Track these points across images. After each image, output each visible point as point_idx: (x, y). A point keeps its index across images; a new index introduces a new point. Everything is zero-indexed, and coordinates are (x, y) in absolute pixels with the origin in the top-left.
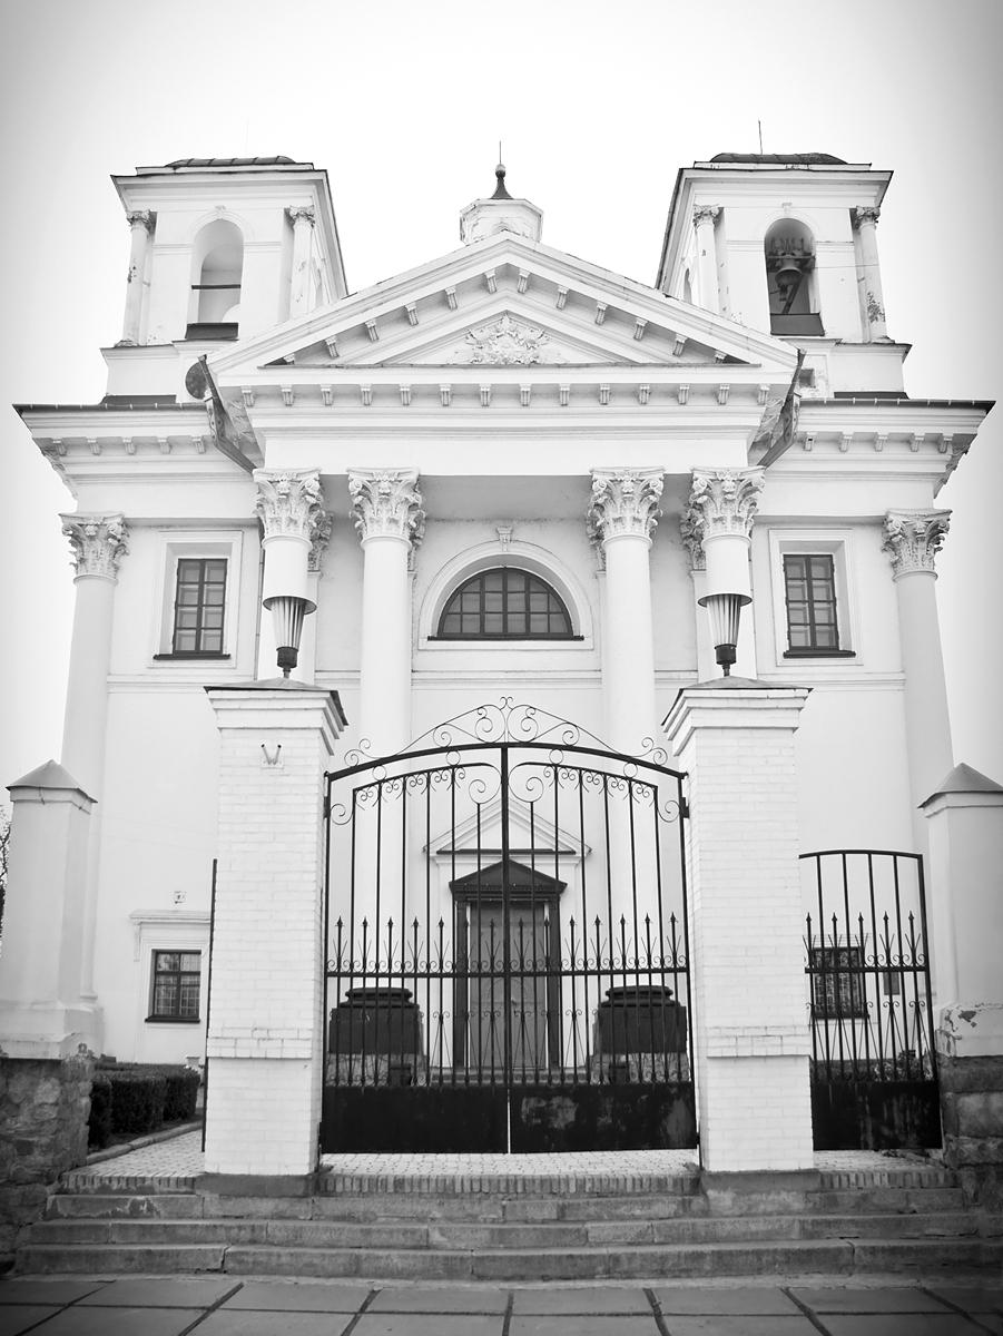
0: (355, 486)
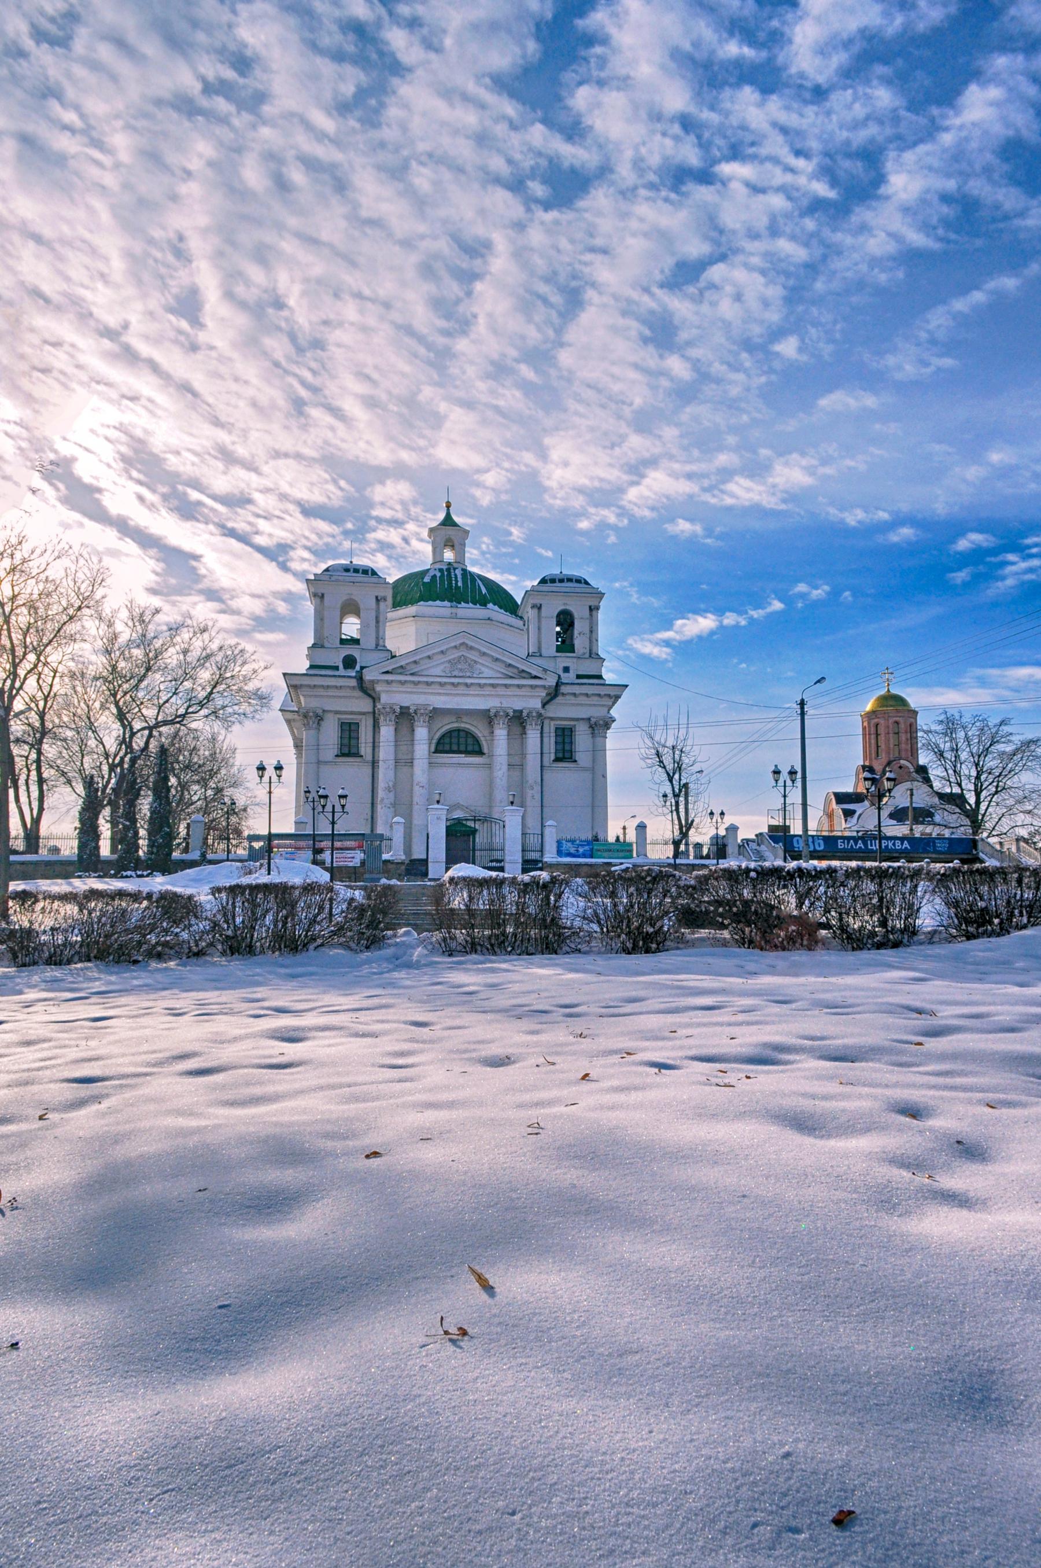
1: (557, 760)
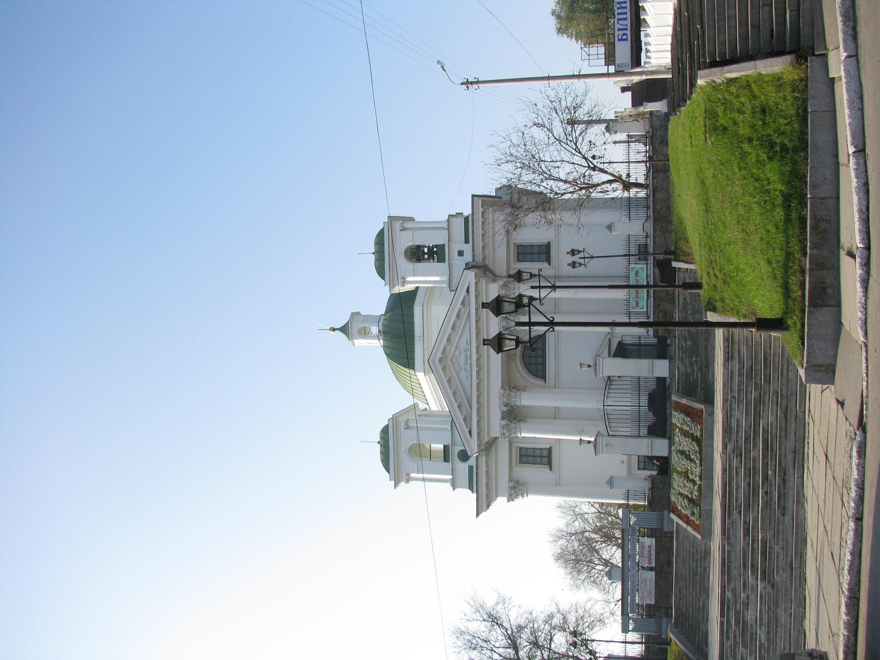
0: (505, 409)
1: (548, 260)
